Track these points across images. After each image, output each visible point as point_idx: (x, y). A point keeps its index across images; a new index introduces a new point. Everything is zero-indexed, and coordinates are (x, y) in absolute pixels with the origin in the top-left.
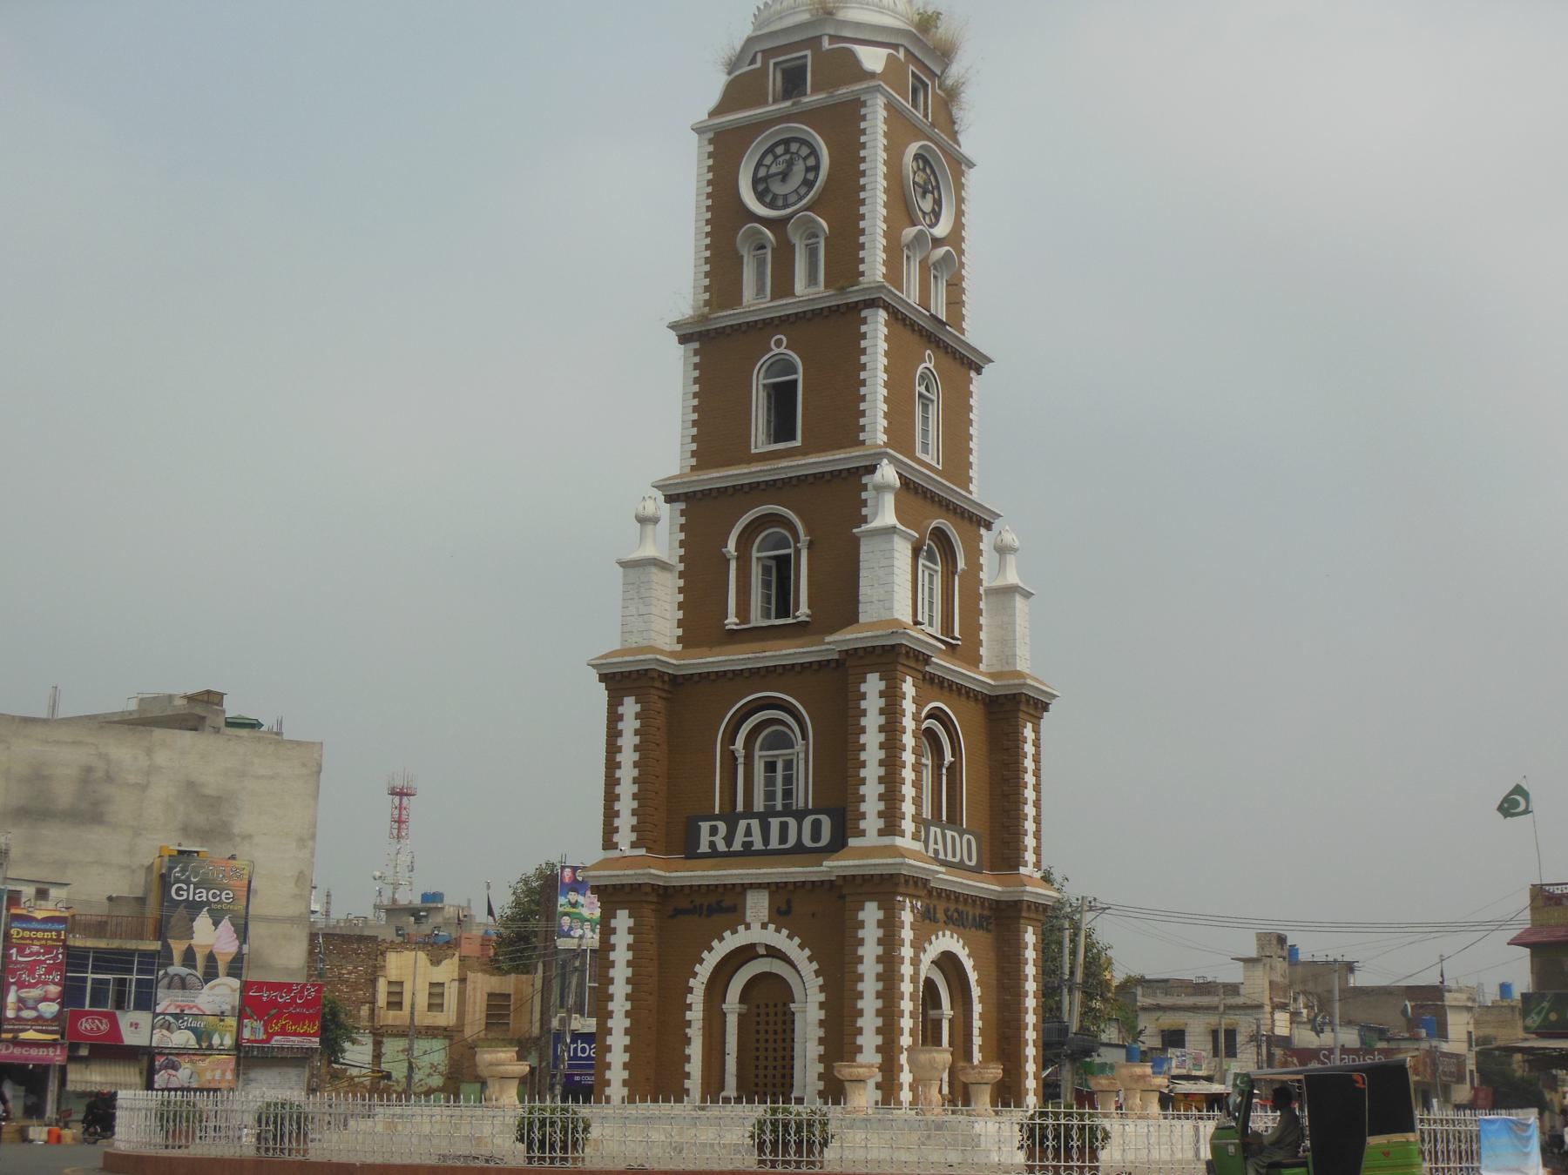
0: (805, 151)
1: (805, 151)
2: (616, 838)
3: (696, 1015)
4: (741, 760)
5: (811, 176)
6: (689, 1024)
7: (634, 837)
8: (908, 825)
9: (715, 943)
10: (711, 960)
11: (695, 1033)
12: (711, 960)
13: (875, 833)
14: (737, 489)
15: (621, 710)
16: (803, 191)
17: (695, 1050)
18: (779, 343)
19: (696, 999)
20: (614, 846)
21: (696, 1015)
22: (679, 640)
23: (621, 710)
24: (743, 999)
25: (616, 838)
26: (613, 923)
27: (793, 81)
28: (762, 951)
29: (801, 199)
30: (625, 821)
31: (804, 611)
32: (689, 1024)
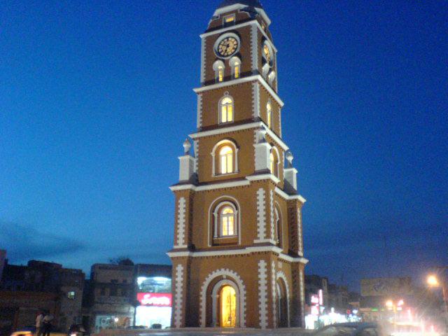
8: (273, 236)
13: (263, 238)
14: (219, 135)
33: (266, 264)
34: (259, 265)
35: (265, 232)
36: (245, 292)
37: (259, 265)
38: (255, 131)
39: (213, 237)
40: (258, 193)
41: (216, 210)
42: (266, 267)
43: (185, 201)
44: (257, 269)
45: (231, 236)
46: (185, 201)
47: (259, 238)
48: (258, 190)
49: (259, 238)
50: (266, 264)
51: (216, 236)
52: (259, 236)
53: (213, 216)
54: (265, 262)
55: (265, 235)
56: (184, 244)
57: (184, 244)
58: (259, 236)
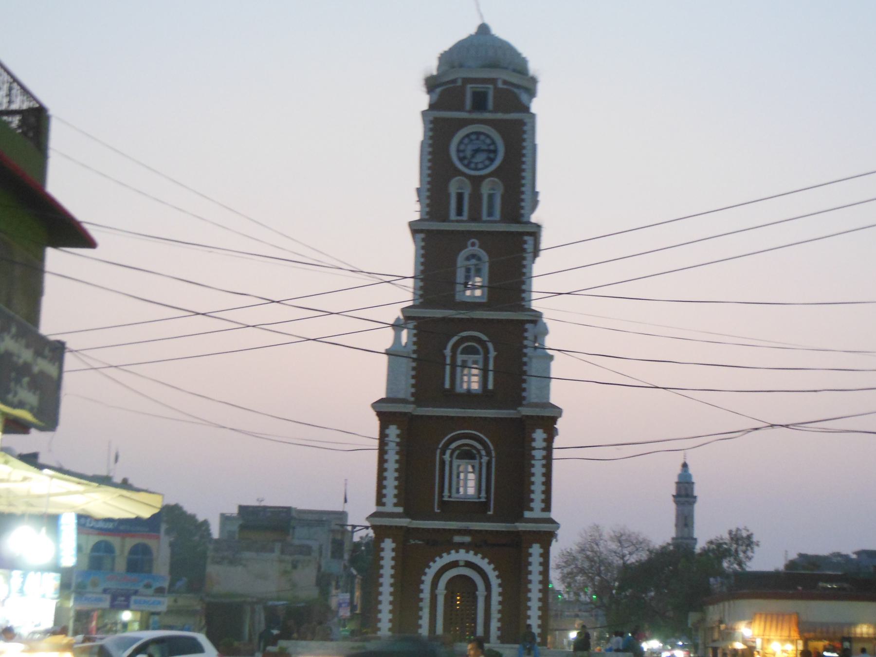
0: (488, 141)
1: (488, 141)
2: (384, 500)
3: (426, 595)
4: (447, 463)
5: (492, 155)
6: (421, 600)
7: (395, 500)
9: (486, 560)
10: (435, 566)
11: (426, 605)
12: (435, 566)
15: (387, 431)
16: (487, 162)
17: (425, 614)
18: (473, 245)
19: (426, 587)
20: (384, 504)
21: (426, 595)
22: (413, 395)
23: (387, 431)
24: (447, 588)
25: (384, 500)
26: (383, 545)
27: (480, 102)
28: (461, 563)
29: (486, 167)
30: (391, 491)
31: (490, 386)
32: (421, 600)
33: (541, 551)
34: (531, 550)
35: (543, 501)
36: (500, 590)
37: (531, 550)
38: (528, 326)
39: (443, 497)
40: (534, 435)
41: (448, 452)
42: (541, 555)
43: (398, 432)
44: (482, 554)
45: (471, 497)
46: (398, 432)
47: (531, 509)
48: (534, 432)
49: (531, 509)
50: (541, 551)
51: (446, 493)
52: (532, 505)
53: (443, 463)
54: (541, 547)
55: (543, 505)
56: (395, 505)
57: (395, 505)
58: (532, 505)
